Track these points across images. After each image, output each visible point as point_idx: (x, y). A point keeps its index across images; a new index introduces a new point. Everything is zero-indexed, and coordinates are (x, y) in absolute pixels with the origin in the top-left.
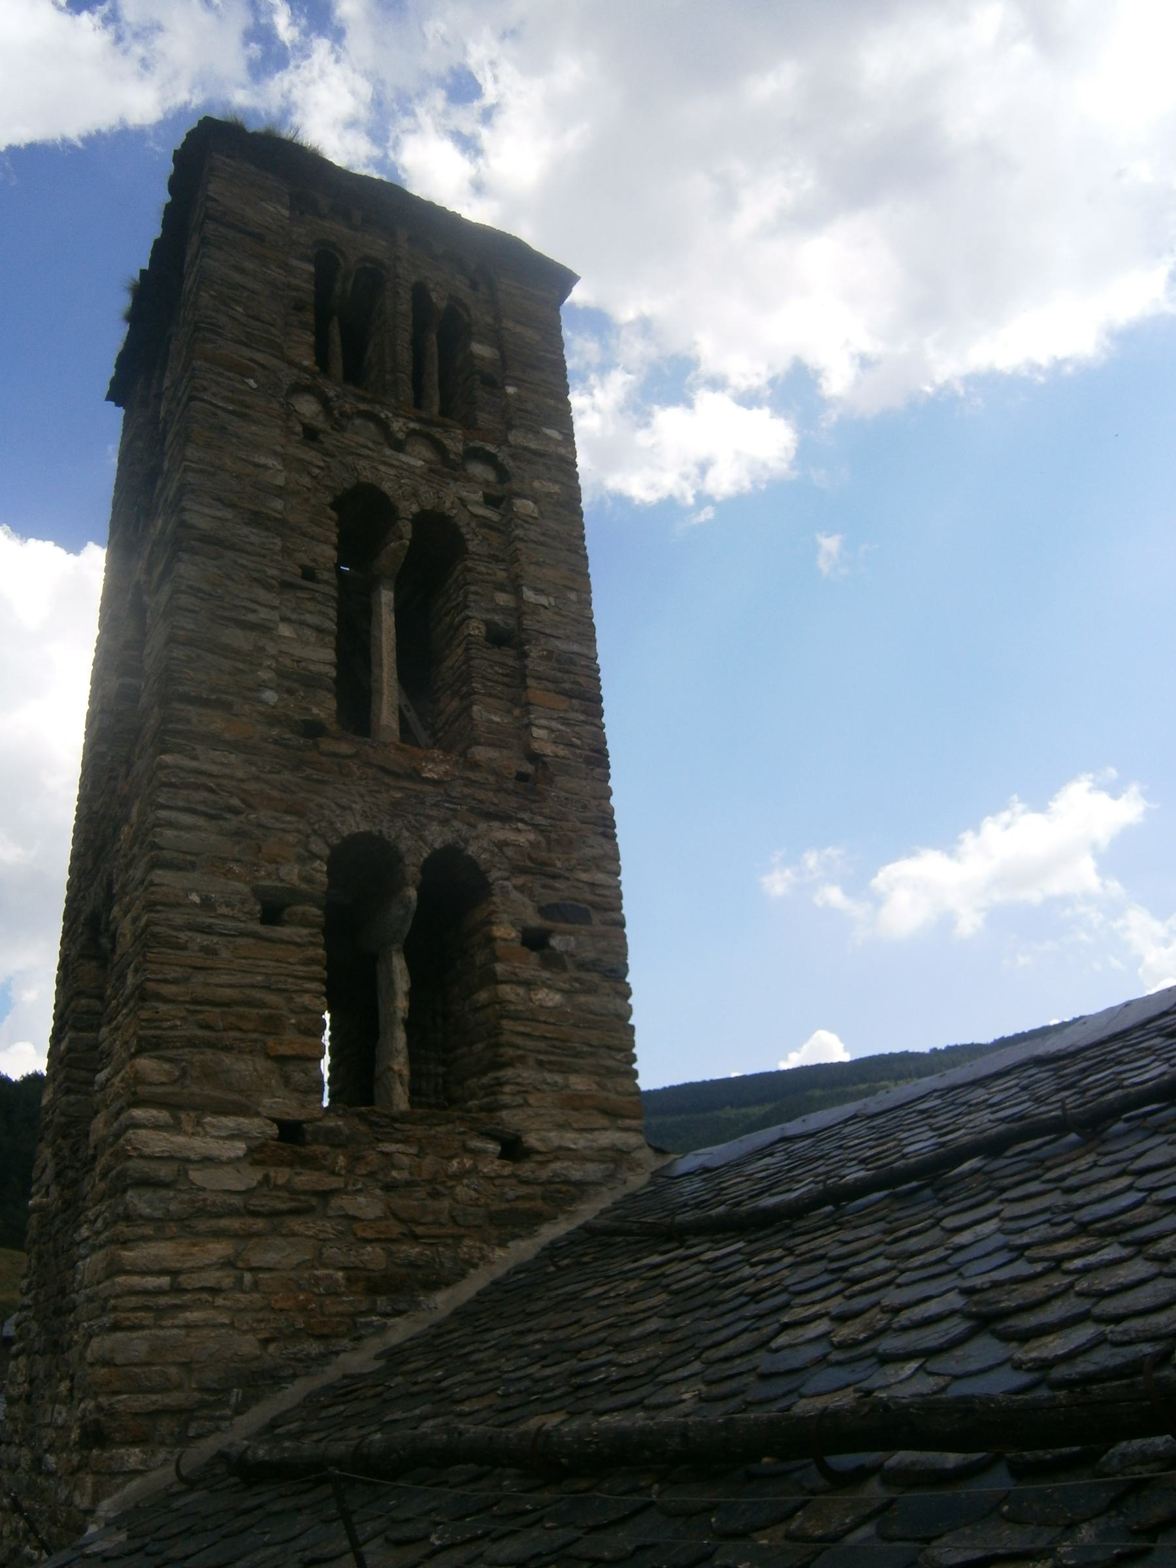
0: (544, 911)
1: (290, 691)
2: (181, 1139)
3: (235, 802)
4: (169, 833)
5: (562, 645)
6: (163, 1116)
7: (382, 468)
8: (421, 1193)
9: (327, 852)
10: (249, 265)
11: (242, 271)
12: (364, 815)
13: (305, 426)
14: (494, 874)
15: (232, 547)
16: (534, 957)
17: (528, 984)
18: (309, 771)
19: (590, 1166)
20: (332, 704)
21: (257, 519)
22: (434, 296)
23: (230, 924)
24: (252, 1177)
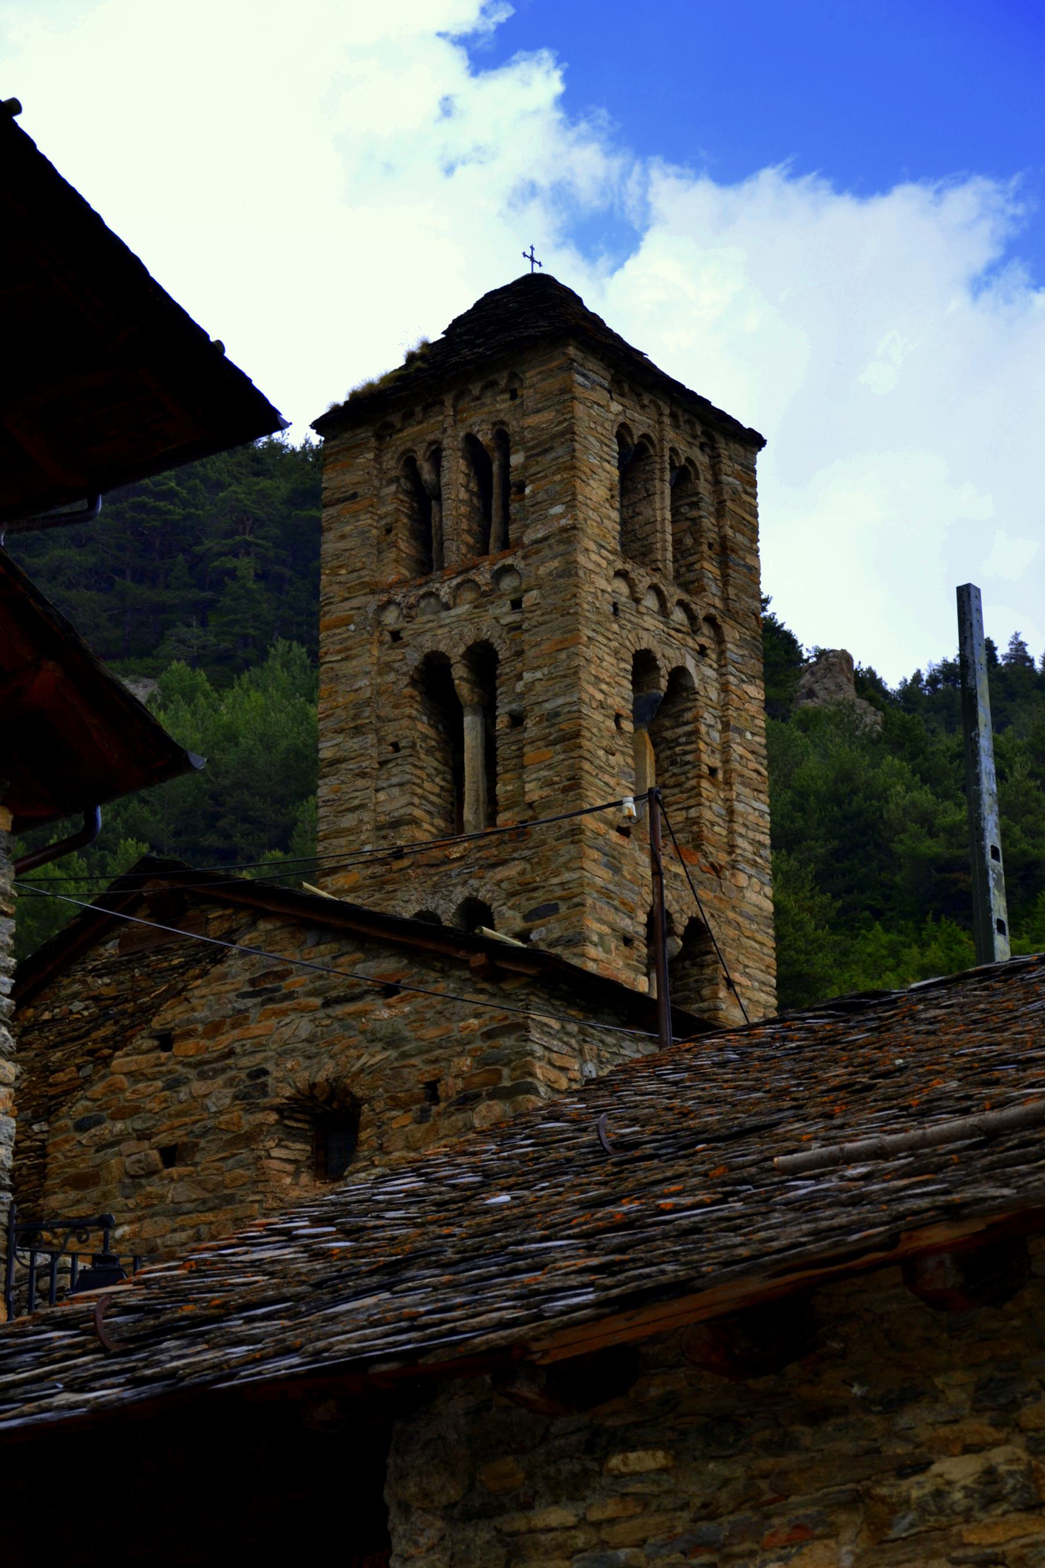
0: (526, 918)
1: (384, 837)
5: (548, 706)
7: (440, 632)
12: (417, 901)
14: (495, 904)
15: (344, 760)
22: (480, 437)
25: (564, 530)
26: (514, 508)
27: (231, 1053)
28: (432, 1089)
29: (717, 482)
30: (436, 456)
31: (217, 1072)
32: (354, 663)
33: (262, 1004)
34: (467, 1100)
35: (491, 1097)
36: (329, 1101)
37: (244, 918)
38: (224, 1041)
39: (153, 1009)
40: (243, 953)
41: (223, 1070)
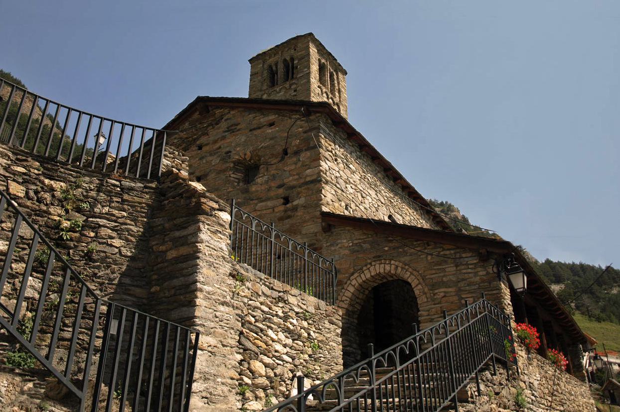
22: (287, 59)
25: (307, 73)
26: (295, 71)
27: (220, 147)
28: (285, 152)
29: (338, 78)
30: (276, 64)
31: (215, 154)
33: (230, 133)
34: (297, 153)
35: (306, 150)
36: (250, 160)
37: (226, 111)
38: (217, 145)
39: (197, 139)
40: (226, 120)
41: (217, 153)
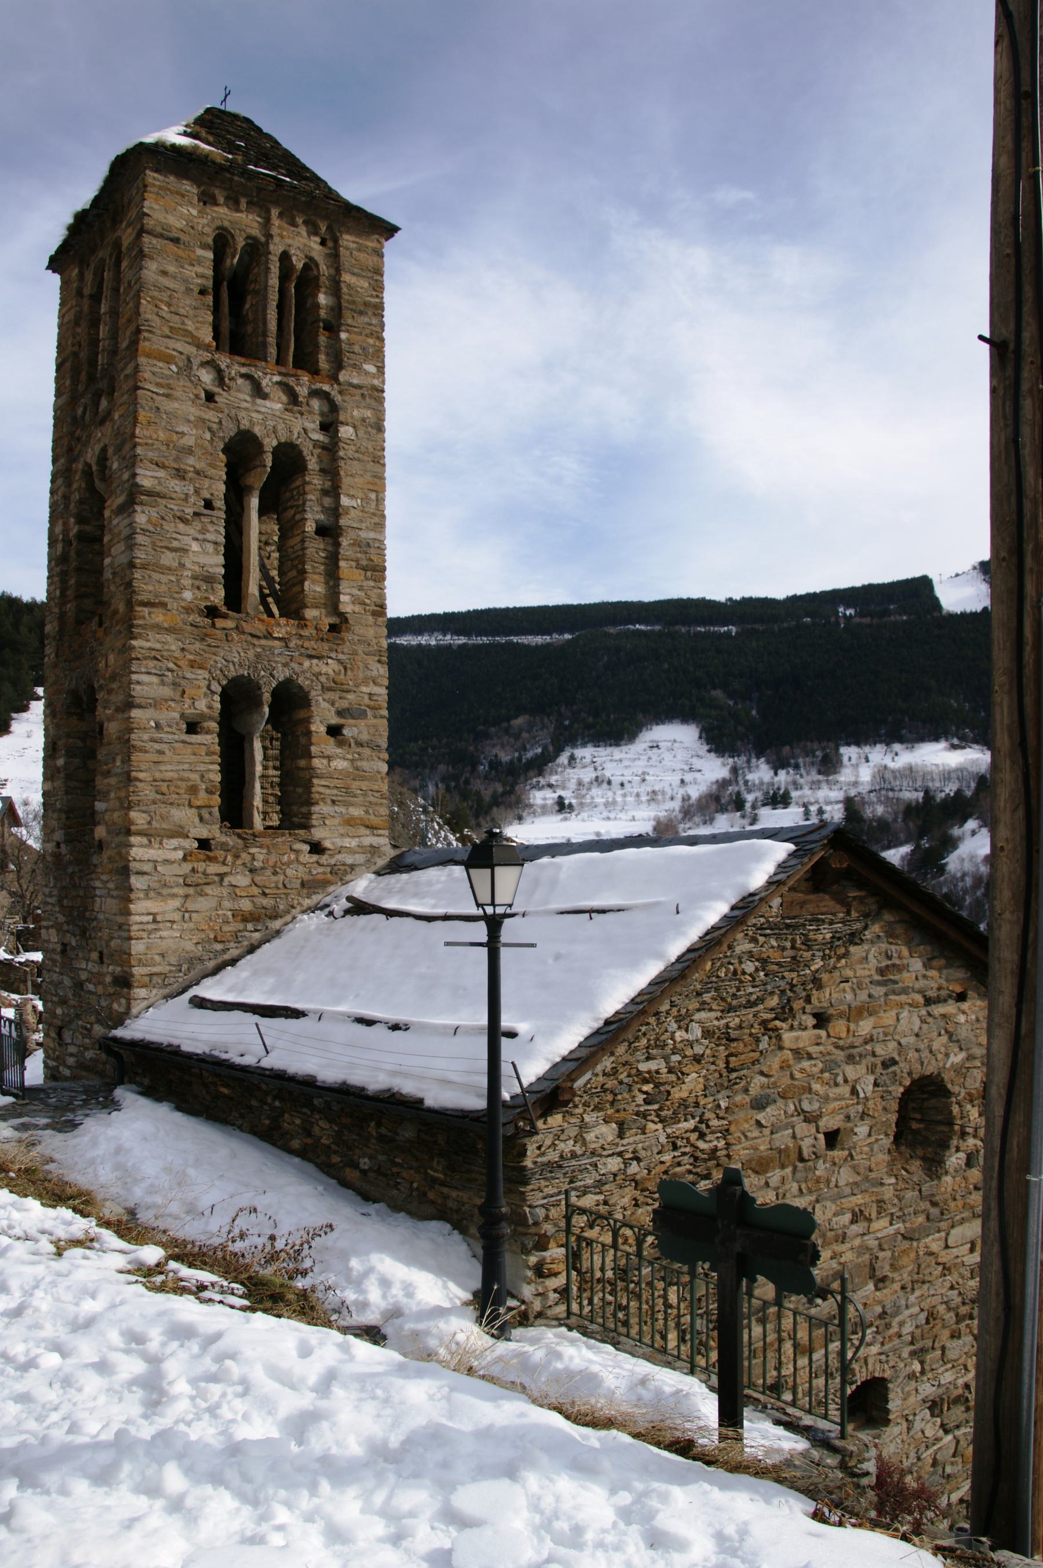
0: (340, 713)
1: (198, 588)
2: (152, 851)
3: (171, 665)
4: (138, 687)
5: (363, 534)
6: (145, 840)
7: (254, 415)
8: (268, 872)
9: (220, 689)
10: (171, 269)
11: (164, 273)
13: (206, 391)
14: (313, 693)
15: (164, 497)
16: (332, 740)
17: (329, 758)
18: (210, 641)
19: (357, 856)
20: (222, 593)
21: (180, 474)
22: (294, 259)
23: (170, 736)
24: (187, 867)
32: (176, 405)
